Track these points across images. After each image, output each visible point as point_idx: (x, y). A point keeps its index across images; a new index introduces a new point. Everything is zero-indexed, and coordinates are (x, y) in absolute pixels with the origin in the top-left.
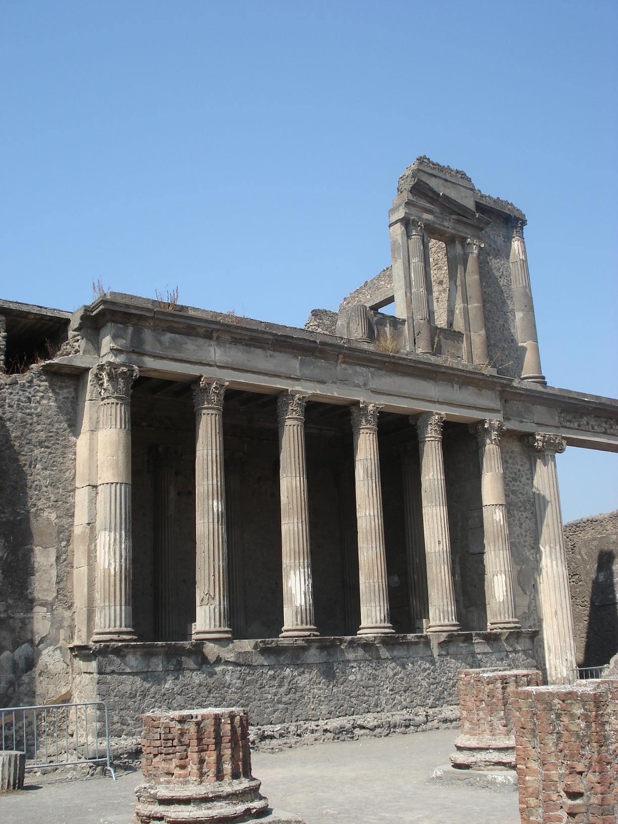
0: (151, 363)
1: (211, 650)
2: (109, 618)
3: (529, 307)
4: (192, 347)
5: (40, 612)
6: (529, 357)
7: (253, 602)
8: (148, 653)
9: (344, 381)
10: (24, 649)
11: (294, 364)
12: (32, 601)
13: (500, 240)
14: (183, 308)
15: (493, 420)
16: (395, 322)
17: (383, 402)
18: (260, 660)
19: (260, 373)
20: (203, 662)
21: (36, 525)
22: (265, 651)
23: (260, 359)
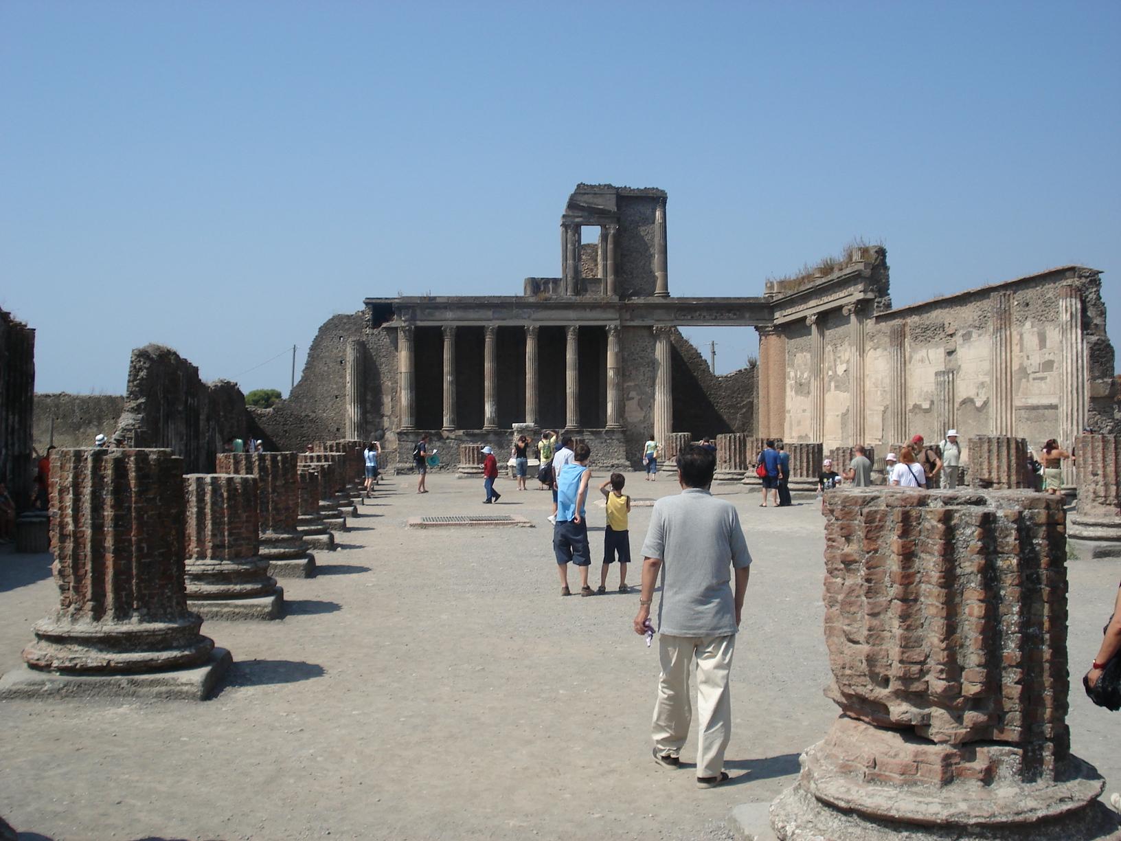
0: (420, 324)
1: (445, 434)
2: (406, 422)
3: (664, 251)
4: (438, 314)
5: (385, 419)
6: (659, 283)
7: (469, 417)
8: (417, 435)
9: (517, 317)
10: (380, 432)
11: (490, 314)
12: (383, 416)
13: (649, 212)
14: (435, 298)
15: (611, 325)
16: (555, 281)
17: (538, 324)
18: (466, 438)
19: (472, 319)
20: (440, 438)
21: (384, 387)
22: (467, 435)
23: (472, 314)
